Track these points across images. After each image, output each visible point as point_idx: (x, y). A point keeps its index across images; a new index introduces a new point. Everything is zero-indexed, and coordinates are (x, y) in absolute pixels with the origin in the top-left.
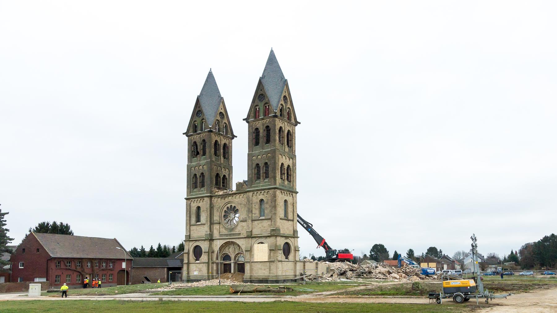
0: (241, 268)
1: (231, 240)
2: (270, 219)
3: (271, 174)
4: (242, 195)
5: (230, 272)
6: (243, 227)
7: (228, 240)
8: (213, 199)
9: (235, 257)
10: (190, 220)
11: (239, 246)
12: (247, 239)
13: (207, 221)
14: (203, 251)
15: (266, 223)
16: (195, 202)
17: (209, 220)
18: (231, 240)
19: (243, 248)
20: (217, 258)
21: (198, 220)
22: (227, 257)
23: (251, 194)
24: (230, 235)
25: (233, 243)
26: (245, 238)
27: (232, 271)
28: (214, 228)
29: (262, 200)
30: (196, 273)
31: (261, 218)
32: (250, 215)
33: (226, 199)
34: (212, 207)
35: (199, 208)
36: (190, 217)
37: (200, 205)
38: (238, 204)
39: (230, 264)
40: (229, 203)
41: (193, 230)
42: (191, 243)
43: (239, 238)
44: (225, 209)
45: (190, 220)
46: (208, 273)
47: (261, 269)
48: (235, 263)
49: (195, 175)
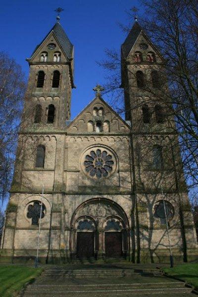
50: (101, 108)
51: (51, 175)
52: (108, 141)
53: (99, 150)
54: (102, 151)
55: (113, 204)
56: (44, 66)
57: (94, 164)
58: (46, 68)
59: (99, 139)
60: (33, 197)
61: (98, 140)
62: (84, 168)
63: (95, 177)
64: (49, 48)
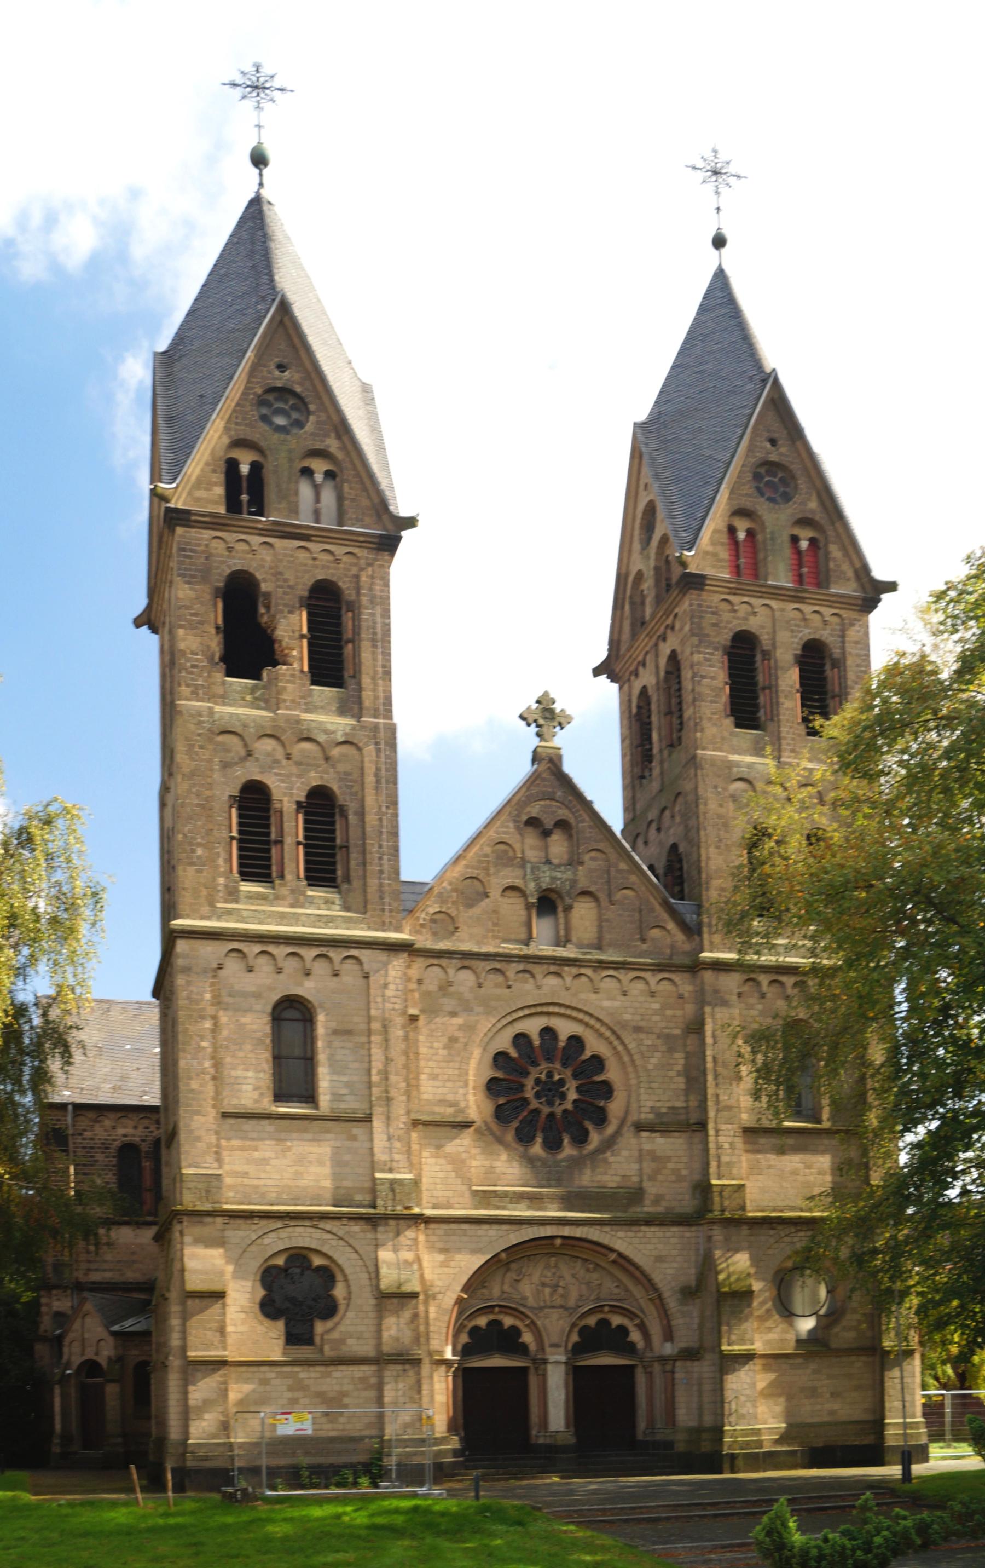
7: (549, 1231)
50: (562, 825)
51: (354, 1138)
52: (596, 991)
53: (548, 1032)
54: (563, 1037)
55: (614, 1262)
56: (256, 540)
57: (529, 1093)
58: (266, 556)
59: (553, 981)
61: (550, 986)
62: (488, 1107)
63: (537, 1149)
64: (264, 418)
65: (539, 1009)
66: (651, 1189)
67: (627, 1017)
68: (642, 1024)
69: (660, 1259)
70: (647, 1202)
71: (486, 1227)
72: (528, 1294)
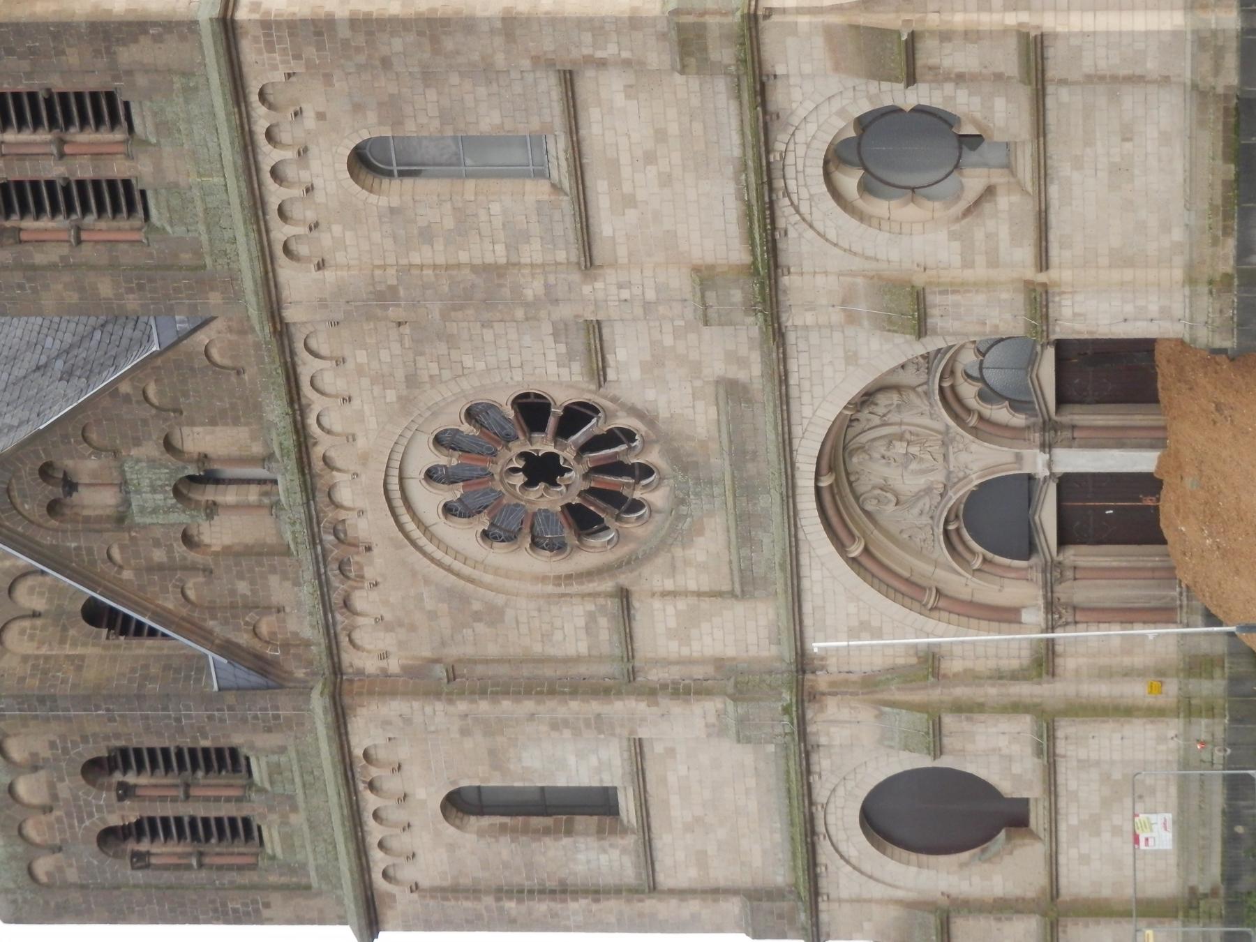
0: (1111, 374)
1: (806, 483)
2: (568, 80)
3: (74, 73)
4: (308, 367)
5: (1149, 484)
6: (655, 362)
8: (371, 665)
9: (985, 430)
10: (596, 892)
11: (867, 398)
12: (794, 319)
13: (600, 724)
14: (925, 762)
15: (619, 119)
16: (402, 842)
17: (595, 706)
18: (806, 483)
19: (885, 352)
20: (1007, 615)
21: (597, 805)
22: (992, 520)
23: (296, 282)
24: (745, 489)
25: (838, 454)
26: (776, 334)
27: (1142, 461)
28: (672, 648)
29: (364, 162)
30: (1159, 833)
31: (560, 170)
32: (533, 288)
33: (361, 528)
34: (443, 680)
35: (460, 804)
36: (563, 891)
37: (430, 796)
38: (406, 403)
39: (1068, 484)
40: (397, 501)
41: (701, 859)
42: (840, 880)
43: (784, 400)
44: (464, 536)
45: (596, 892)
46: (1154, 713)
47: (1121, 171)
48: (1051, 434)
49: (109, 837)
60: (839, 836)
65: (398, 503)
66: (717, 367)
67: (391, 396)
68: (400, 374)
69: (851, 358)
70: (742, 376)
71: (806, 583)
72: (922, 482)
